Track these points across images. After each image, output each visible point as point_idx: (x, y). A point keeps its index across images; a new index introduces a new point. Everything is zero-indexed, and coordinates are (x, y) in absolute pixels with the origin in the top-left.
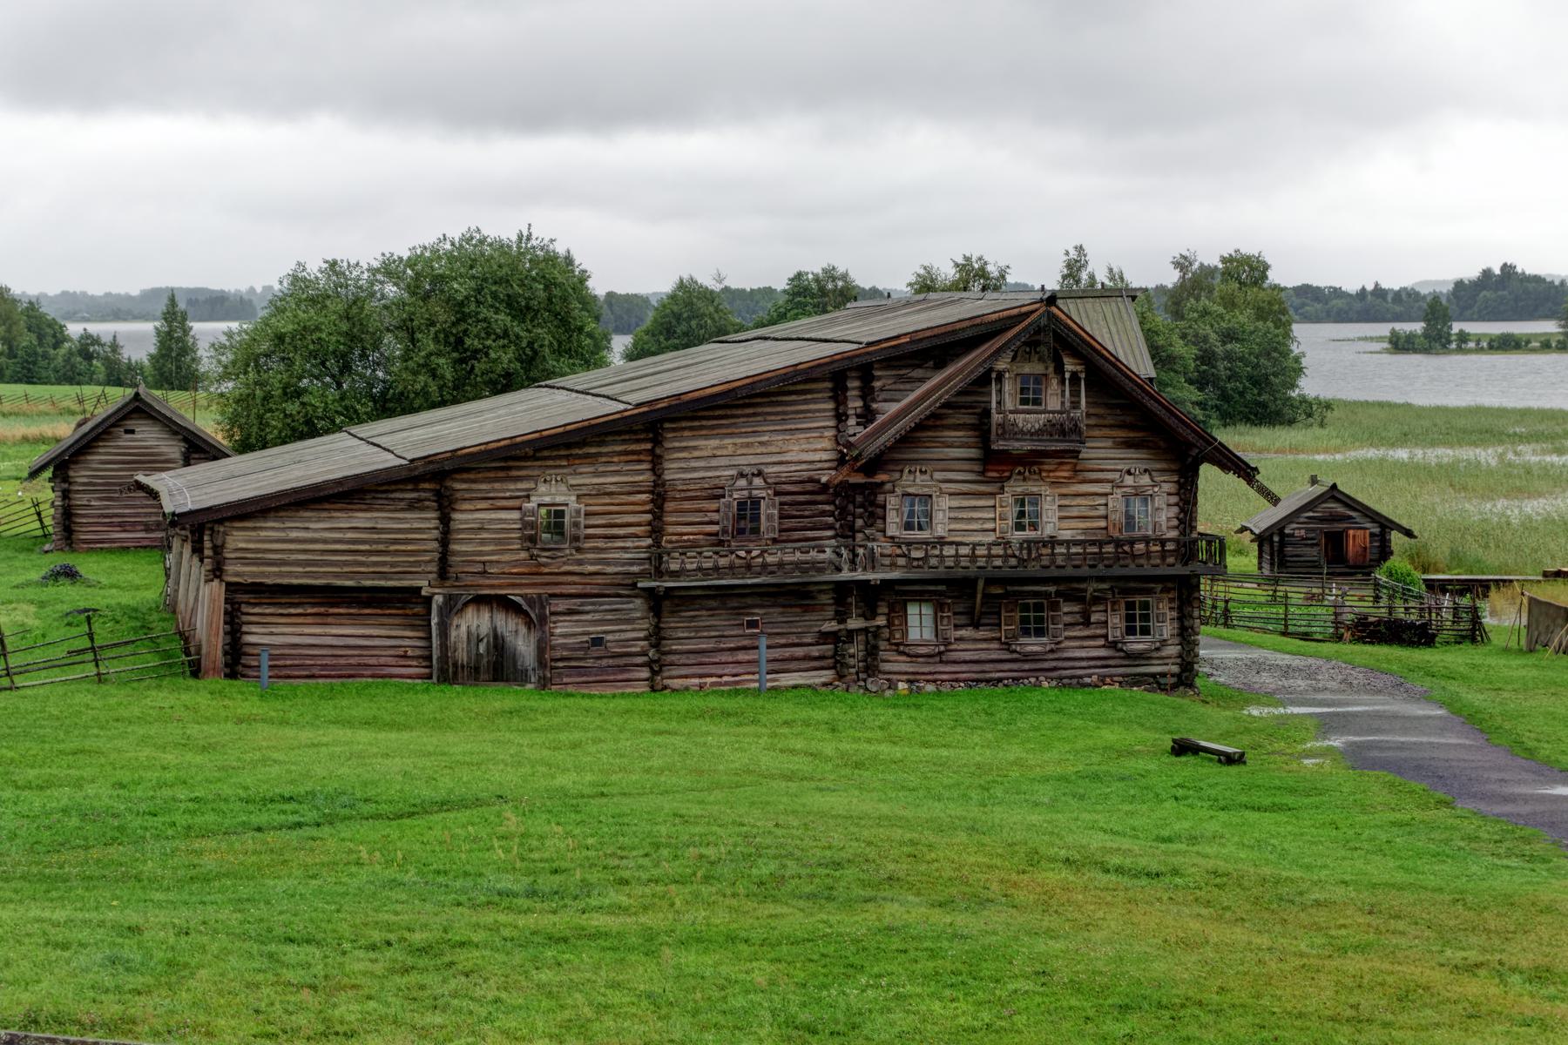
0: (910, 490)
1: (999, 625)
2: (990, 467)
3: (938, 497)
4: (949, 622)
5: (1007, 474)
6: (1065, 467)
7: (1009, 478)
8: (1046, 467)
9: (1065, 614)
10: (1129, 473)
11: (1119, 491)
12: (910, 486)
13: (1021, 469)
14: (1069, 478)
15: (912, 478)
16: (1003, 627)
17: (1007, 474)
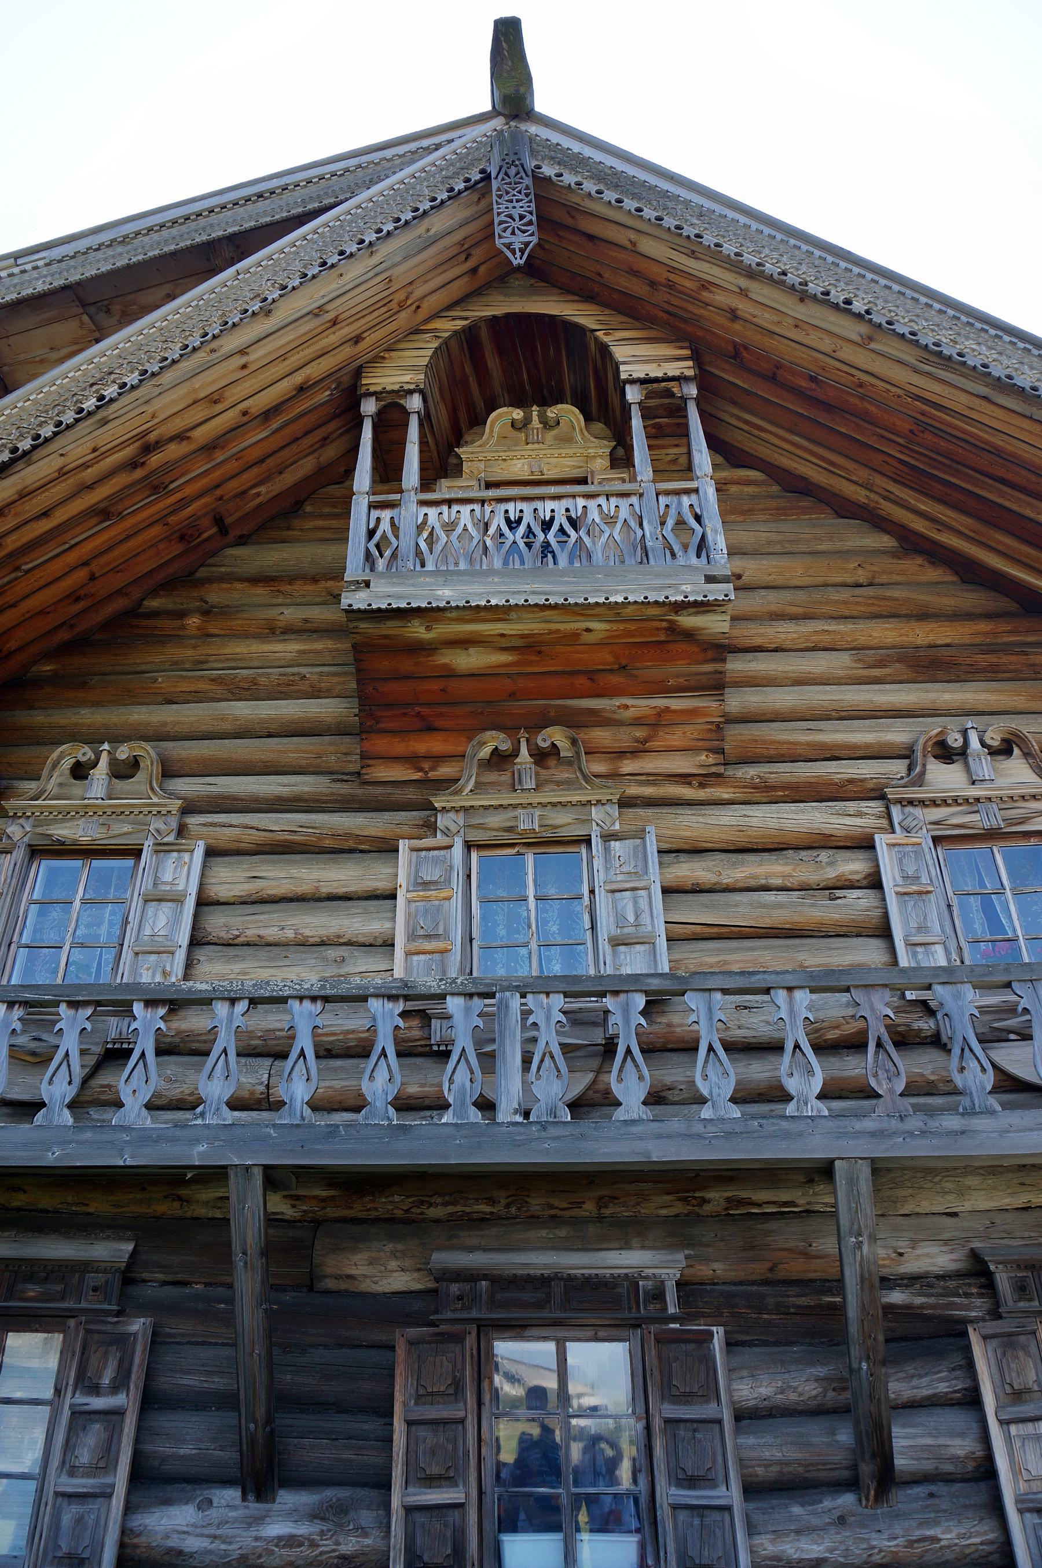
0: (63, 831)
1: (385, 1485)
2: (381, 744)
3: (162, 849)
4: (106, 1461)
5: (445, 771)
6: (676, 737)
7: (449, 783)
8: (601, 736)
9: (744, 1416)
10: (945, 753)
11: (918, 812)
12: (65, 815)
13: (493, 741)
14: (705, 780)
15: (77, 788)
16: (396, 1501)
17: (445, 771)
